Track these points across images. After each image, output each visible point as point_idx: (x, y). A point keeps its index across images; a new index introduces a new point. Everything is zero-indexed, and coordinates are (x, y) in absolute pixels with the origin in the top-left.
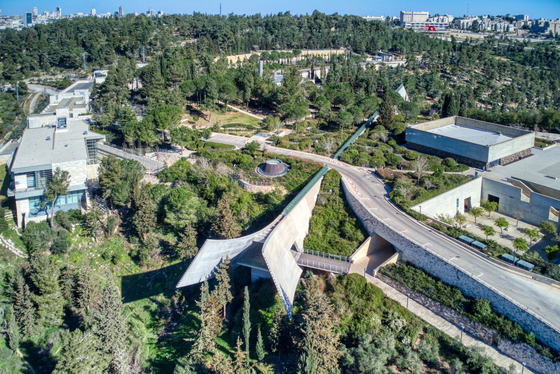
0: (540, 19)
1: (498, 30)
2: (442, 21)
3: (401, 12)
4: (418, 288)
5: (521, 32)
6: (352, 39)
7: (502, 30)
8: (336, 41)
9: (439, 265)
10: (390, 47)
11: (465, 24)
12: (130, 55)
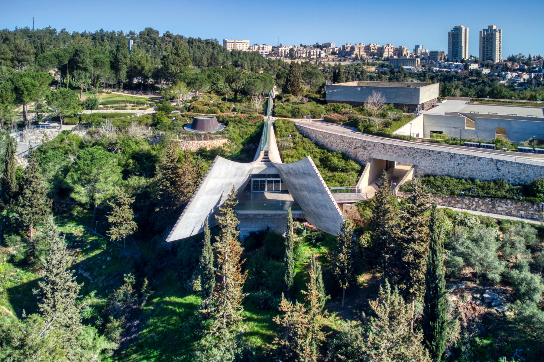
0: (347, 44)
1: (312, 57)
4: (457, 192)
5: (331, 57)
7: (315, 57)
9: (470, 164)
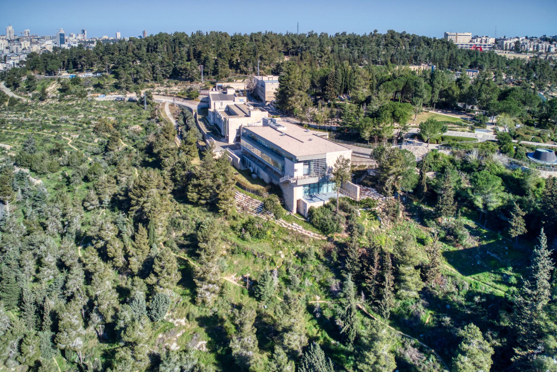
1: (540, 51)
2: (486, 42)
3: (445, 33)
6: (432, 56)
7: (544, 51)
8: (418, 57)
10: (469, 64)
11: (508, 45)
12: (245, 69)
